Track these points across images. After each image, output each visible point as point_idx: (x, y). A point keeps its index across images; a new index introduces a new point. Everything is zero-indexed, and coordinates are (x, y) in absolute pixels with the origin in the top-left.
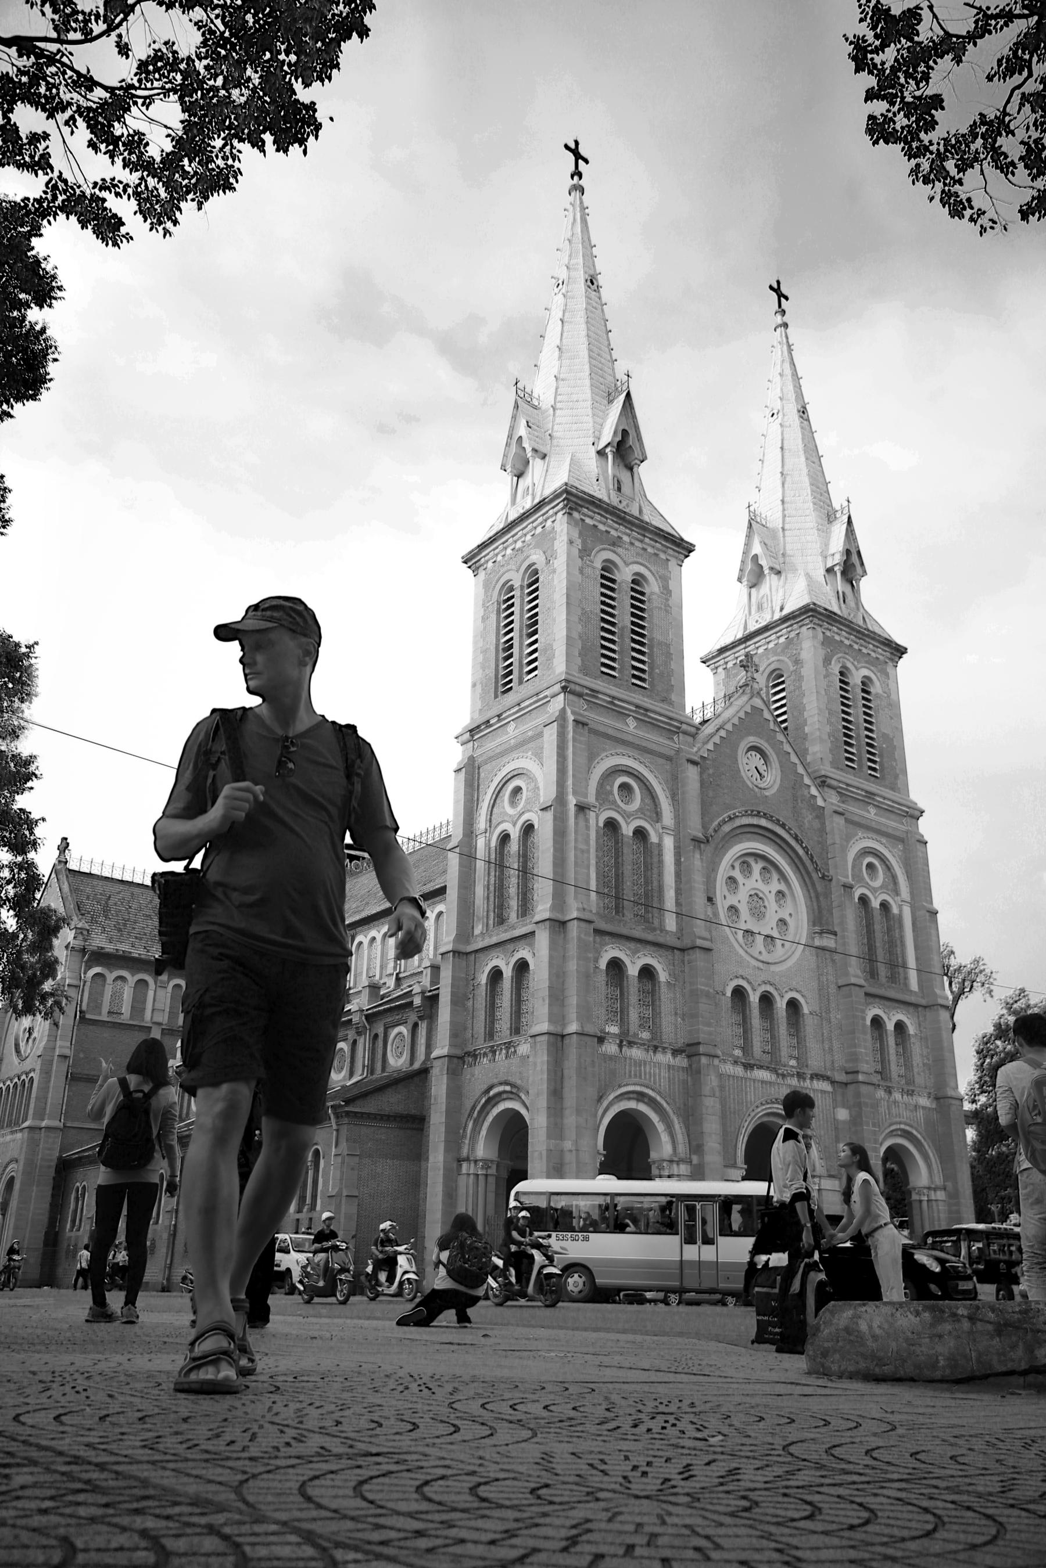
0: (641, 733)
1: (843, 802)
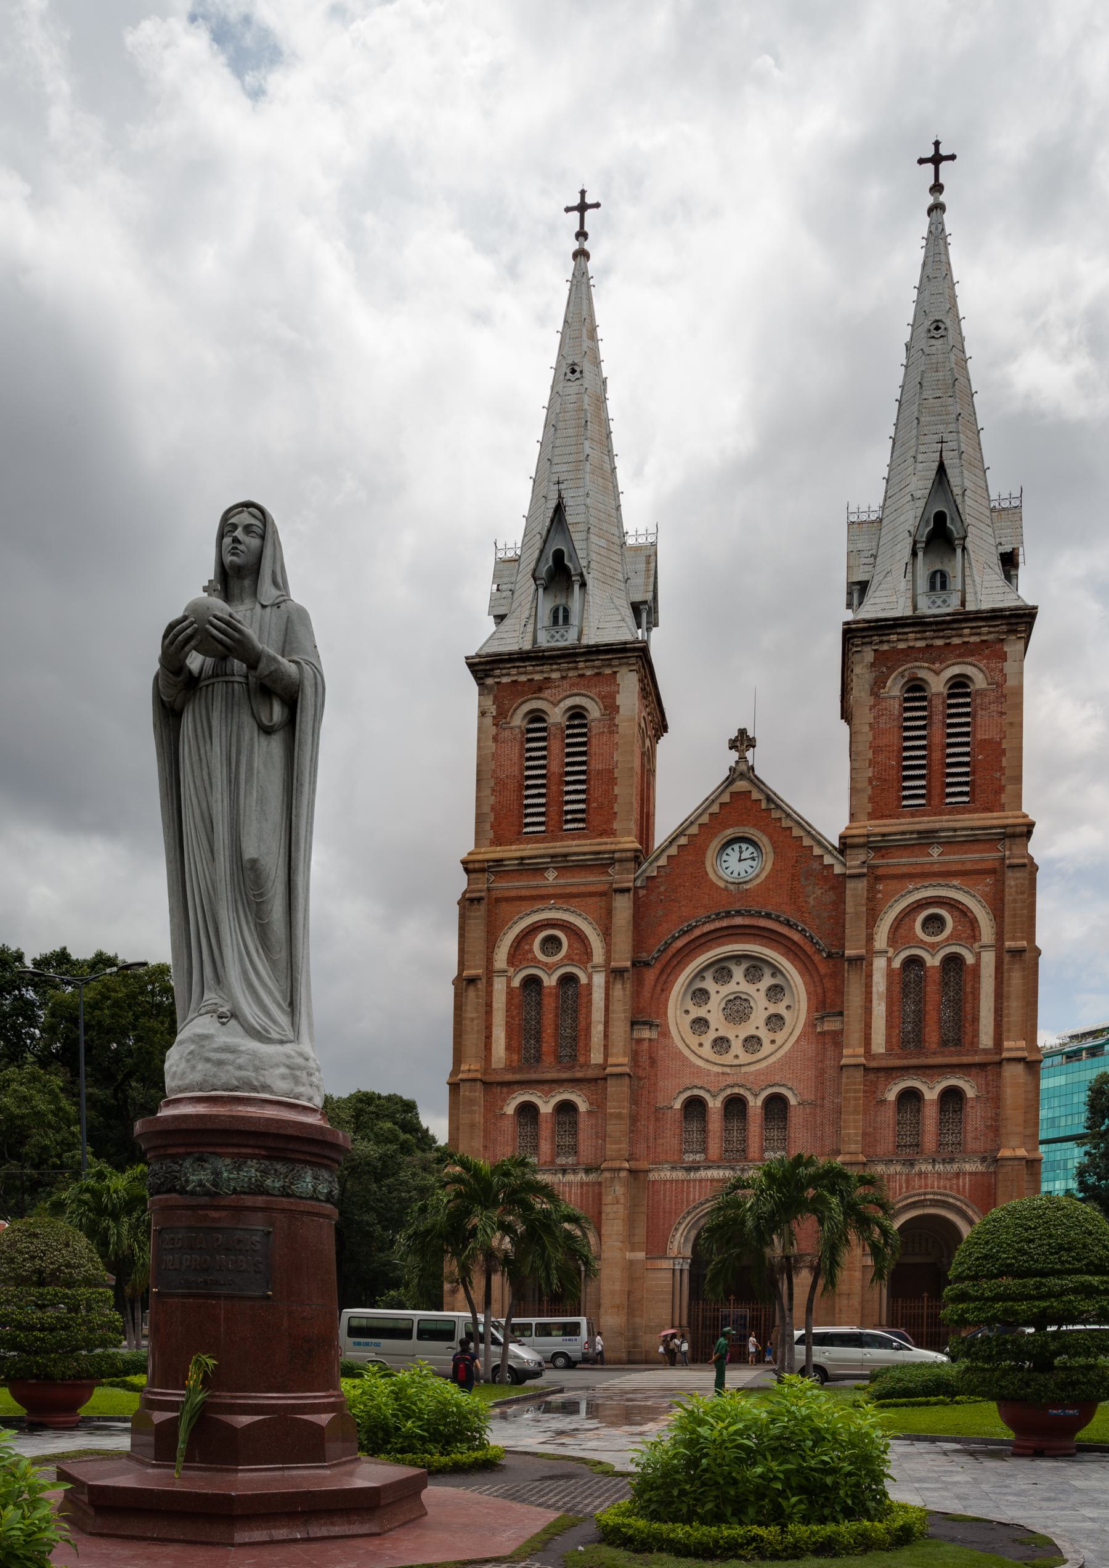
0: (562, 881)
1: (883, 857)
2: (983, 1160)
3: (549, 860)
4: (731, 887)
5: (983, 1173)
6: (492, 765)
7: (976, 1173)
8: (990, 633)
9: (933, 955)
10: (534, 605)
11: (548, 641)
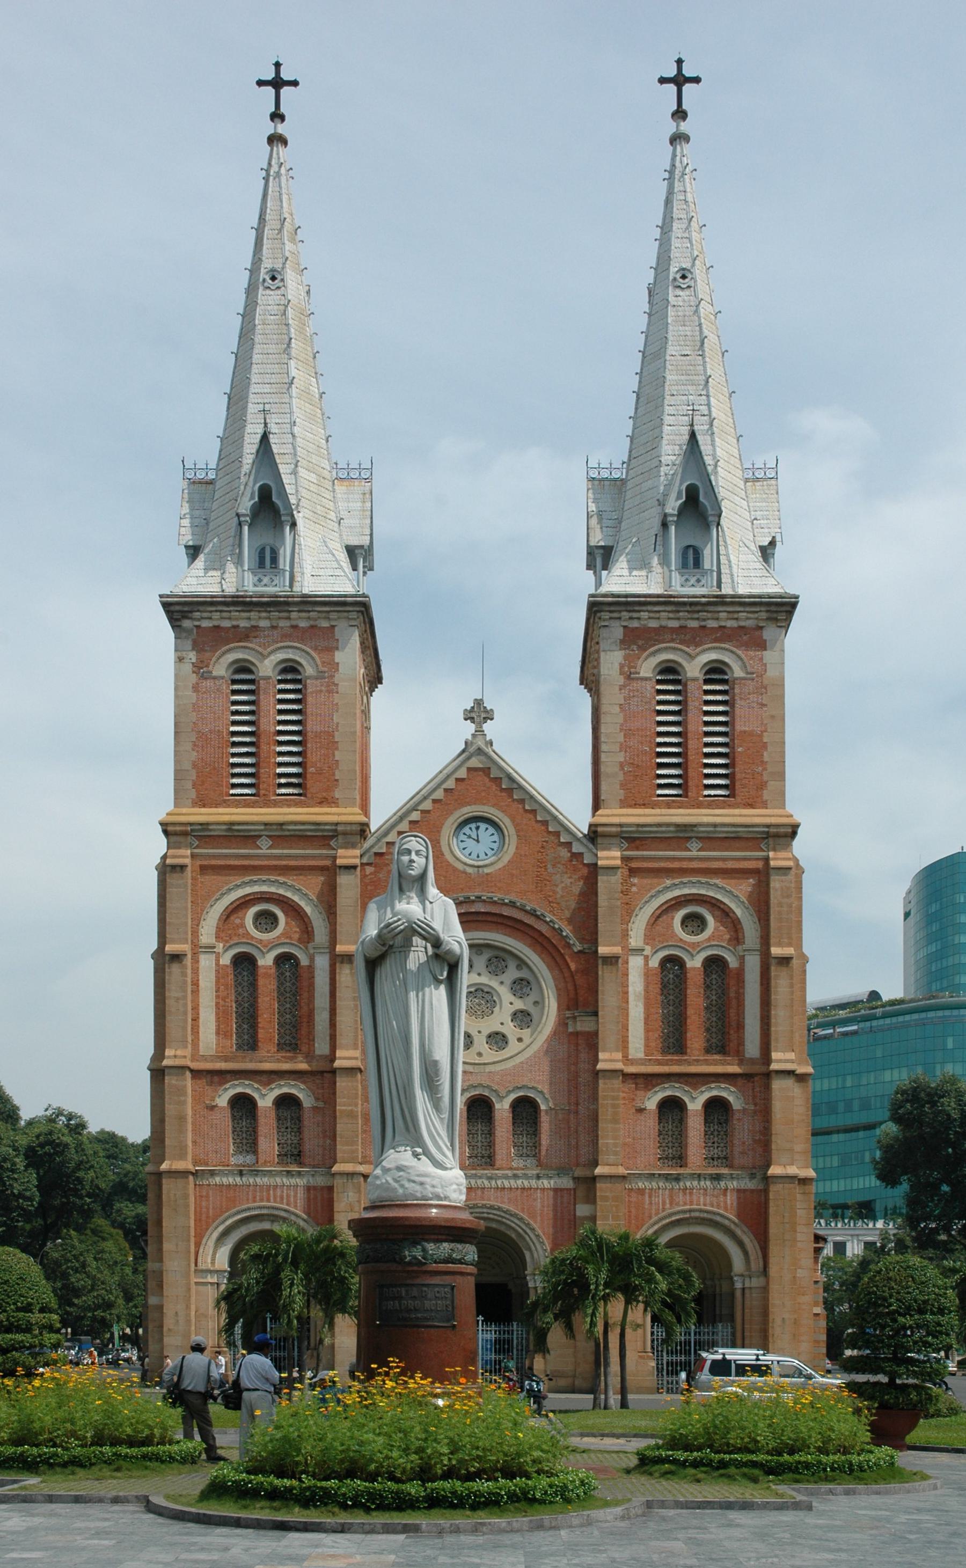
1: (637, 849)
2: (752, 1176)
3: (262, 827)
4: (469, 870)
5: (752, 1191)
6: (193, 717)
7: (745, 1191)
8: (748, 618)
9: (692, 956)
10: (237, 542)
11: (255, 585)
